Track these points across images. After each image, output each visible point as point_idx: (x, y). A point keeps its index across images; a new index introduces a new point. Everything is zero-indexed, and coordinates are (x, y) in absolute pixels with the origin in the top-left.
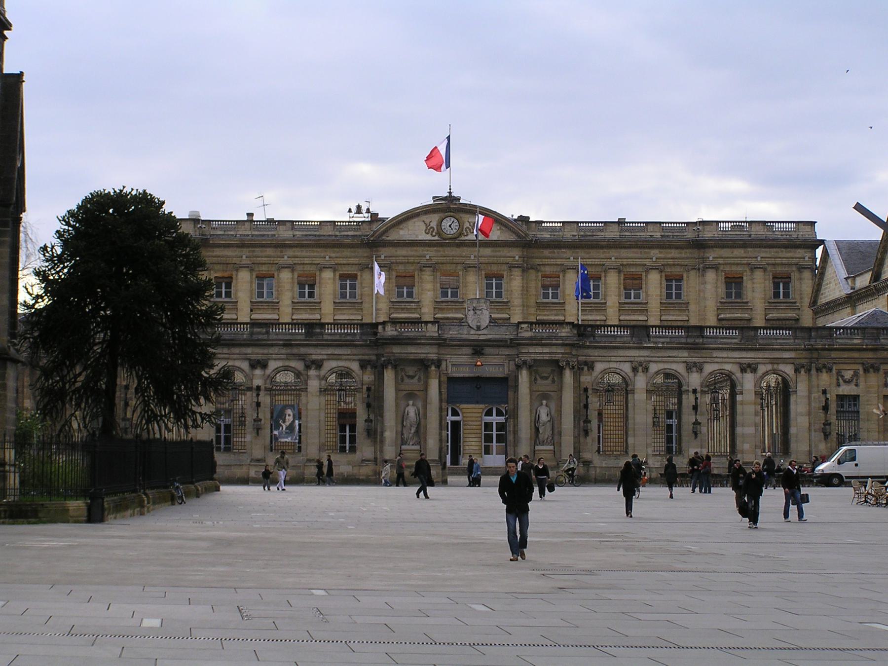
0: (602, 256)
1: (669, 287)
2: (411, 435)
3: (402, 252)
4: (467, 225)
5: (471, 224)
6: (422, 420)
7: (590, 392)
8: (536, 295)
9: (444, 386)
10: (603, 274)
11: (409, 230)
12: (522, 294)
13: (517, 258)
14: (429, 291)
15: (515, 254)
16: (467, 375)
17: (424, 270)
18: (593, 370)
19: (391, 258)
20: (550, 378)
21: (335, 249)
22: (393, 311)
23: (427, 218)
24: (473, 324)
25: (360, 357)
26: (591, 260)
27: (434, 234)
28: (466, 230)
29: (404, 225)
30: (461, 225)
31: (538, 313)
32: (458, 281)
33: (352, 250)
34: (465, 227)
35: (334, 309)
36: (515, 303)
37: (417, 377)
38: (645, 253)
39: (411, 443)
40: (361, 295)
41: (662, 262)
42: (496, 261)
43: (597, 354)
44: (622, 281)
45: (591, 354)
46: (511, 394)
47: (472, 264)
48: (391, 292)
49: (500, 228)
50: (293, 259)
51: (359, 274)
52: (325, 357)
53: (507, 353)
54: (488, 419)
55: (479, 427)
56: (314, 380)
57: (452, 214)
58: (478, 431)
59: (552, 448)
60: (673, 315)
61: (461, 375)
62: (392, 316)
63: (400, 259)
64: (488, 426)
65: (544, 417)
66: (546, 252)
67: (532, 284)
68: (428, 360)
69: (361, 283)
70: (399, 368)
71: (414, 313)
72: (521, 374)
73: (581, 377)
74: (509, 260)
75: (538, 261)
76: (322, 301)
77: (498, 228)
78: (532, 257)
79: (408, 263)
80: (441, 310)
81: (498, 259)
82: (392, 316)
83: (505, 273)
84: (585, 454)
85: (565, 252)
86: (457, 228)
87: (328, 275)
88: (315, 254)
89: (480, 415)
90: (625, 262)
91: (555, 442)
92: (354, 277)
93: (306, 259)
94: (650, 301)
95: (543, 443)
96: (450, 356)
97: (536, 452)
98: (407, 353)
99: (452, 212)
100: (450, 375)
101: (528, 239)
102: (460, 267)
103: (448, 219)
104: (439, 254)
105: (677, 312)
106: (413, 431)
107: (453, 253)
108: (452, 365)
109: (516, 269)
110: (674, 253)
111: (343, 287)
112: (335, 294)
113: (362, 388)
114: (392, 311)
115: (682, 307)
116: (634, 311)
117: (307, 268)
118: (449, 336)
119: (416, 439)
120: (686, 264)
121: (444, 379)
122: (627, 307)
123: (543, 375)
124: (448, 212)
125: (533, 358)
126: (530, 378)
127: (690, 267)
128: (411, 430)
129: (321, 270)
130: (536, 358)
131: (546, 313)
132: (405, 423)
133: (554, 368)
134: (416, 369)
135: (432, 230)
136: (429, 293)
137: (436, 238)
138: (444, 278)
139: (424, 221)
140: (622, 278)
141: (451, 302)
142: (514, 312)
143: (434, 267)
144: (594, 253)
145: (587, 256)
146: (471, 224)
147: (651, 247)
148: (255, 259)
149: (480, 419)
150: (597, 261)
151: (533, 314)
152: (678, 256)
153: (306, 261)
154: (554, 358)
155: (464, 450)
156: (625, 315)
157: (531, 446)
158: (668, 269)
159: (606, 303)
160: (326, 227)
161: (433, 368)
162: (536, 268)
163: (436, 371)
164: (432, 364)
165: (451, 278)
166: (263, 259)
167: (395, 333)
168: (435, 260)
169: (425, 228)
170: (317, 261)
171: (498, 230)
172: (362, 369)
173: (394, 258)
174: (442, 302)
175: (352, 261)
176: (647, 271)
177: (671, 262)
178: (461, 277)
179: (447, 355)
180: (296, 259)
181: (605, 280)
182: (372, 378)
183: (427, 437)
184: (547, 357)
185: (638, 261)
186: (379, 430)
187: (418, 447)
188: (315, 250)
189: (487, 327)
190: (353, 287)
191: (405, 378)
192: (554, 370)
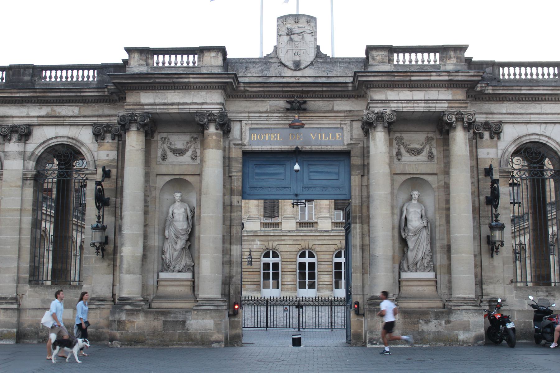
2: (176, 254)
6: (197, 228)
7: (496, 176)
9: (237, 166)
16: (276, 147)
18: (499, 138)
20: (425, 153)
24: (287, 59)
25: (95, 120)
37: (189, 153)
39: (177, 268)
43: (504, 111)
45: (495, 112)
46: (355, 179)
52: (35, 121)
53: (348, 108)
55: (330, 266)
56: (14, 159)
58: (330, 270)
59: (431, 275)
61: (267, 147)
65: (415, 222)
68: (201, 114)
70: (158, 137)
72: (374, 140)
73: (479, 150)
84: (491, 286)
89: (331, 256)
91: (438, 264)
95: (415, 267)
96: (247, 115)
97: (403, 283)
98: (165, 104)
100: (248, 148)
106: (179, 246)
108: (250, 129)
113: (96, 174)
118: (247, 80)
119: (185, 261)
121: (236, 153)
123: (412, 146)
125: (393, 109)
126: (390, 152)
128: (176, 243)
130: (401, 110)
132: (167, 233)
133: (429, 135)
134: (187, 138)
149: (330, 260)
154: (433, 110)
155: (318, 285)
157: (393, 272)
161: (212, 129)
163: (216, 134)
164: (210, 121)
167: (144, 69)
172: (97, 141)
179: (241, 112)
182: (113, 155)
183: (201, 255)
184: (420, 108)
186: (119, 244)
187: (188, 275)
189: (312, 64)
191: (169, 154)
192: (432, 138)
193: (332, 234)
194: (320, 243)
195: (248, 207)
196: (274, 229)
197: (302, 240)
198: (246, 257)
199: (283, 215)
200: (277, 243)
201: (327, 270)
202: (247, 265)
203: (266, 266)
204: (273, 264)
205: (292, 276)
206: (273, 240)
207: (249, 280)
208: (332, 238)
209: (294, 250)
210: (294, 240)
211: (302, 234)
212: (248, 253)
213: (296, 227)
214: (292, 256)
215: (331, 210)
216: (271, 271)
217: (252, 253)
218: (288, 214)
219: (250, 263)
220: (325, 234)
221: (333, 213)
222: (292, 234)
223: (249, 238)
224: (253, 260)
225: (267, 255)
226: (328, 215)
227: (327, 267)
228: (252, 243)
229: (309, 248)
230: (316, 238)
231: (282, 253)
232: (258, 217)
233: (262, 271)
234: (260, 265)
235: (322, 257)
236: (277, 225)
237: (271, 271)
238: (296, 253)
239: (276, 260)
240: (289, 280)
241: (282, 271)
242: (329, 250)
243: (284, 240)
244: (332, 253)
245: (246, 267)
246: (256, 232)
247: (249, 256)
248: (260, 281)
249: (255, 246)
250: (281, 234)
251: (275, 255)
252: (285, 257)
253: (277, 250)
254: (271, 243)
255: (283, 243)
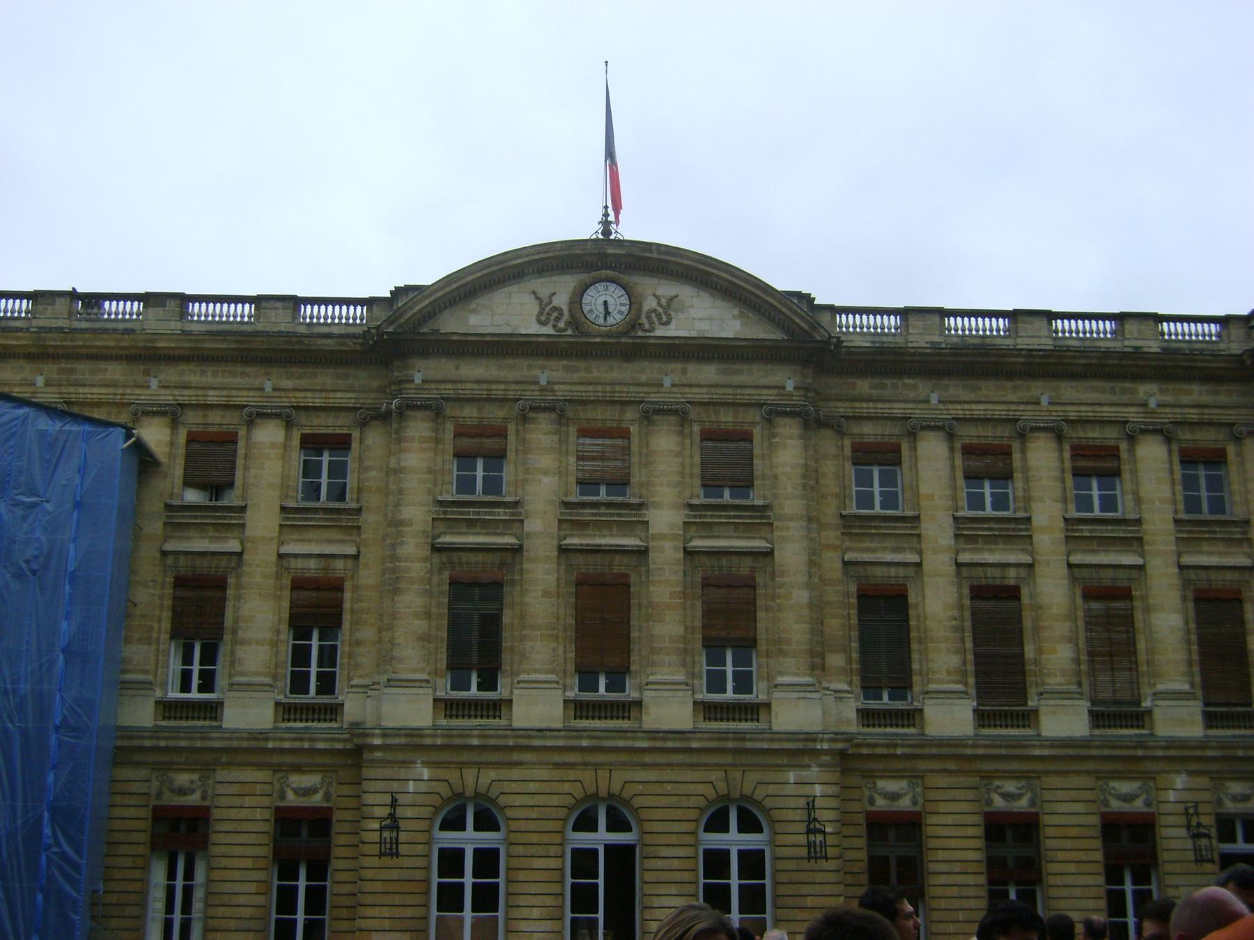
0: (1011, 397)
1: (1190, 483)
3: (473, 370)
4: (650, 304)
5: (663, 301)
8: (838, 496)
10: (1016, 445)
11: (493, 315)
12: (804, 486)
13: (790, 386)
14: (546, 473)
15: (787, 380)
17: (534, 418)
19: (442, 386)
21: (294, 370)
22: (441, 529)
23: (543, 286)
26: (981, 407)
27: (561, 325)
28: (648, 317)
29: (481, 301)
30: (634, 301)
31: (847, 544)
32: (626, 451)
33: (341, 371)
34: (646, 308)
35: (281, 525)
36: (788, 510)
38: (1123, 391)
40: (360, 490)
41: (1169, 414)
42: (730, 398)
44: (1068, 464)
47: (664, 403)
48: (440, 477)
49: (742, 312)
50: (176, 392)
51: (356, 434)
54: (715, 840)
57: (610, 273)
58: (687, 876)
60: (1211, 553)
62: (439, 540)
63: (469, 389)
64: (716, 862)
66: (863, 386)
67: (829, 468)
69: (360, 459)
71: (503, 534)
74: (768, 396)
75: (842, 408)
76: (249, 502)
77: (736, 312)
78: (827, 399)
79: (490, 400)
80: (581, 526)
81: (739, 391)
82: (439, 540)
83: (757, 432)
85: (914, 387)
86: (625, 309)
87: (269, 435)
88: (238, 380)
90: (1073, 412)
92: (341, 443)
93: (211, 393)
94: (1146, 516)
99: (611, 268)
101: (819, 338)
102: (631, 414)
103: (600, 286)
104: (576, 377)
105: (1221, 547)
107: (615, 375)
109: (787, 420)
110: (1196, 393)
111: (310, 469)
112: (284, 486)
114: (441, 527)
115: (1231, 532)
116: (1107, 543)
117: (215, 418)
120: (1232, 419)
122: (1086, 531)
124: (602, 268)
127: (1244, 429)
129: (251, 423)
131: (867, 545)
135: (555, 314)
136: (545, 480)
137: (569, 332)
138: (588, 441)
139: (534, 293)
140: (1067, 455)
141: (609, 505)
142: (783, 533)
143: (559, 410)
144: (989, 389)
145: (972, 397)
146: (663, 301)
147: (1141, 376)
148: (71, 390)
149: (689, 839)
150: (999, 411)
151: (835, 548)
152: (1207, 399)
153: (213, 397)
156: (1085, 551)
158: (1186, 435)
159: (1029, 519)
160: (273, 313)
162: (835, 426)
165: (608, 442)
166: (95, 390)
168: (562, 391)
169: (535, 309)
170: (243, 398)
171: (734, 317)
173: (450, 386)
174: (583, 505)
175: (340, 398)
176: (1132, 439)
177: (1193, 415)
178: (635, 438)
180: (187, 392)
181: (1024, 459)
185: (1107, 413)
188: (239, 369)
190: (338, 470)
193: (695, 745)
194: (651, 775)
195: (392, 642)
196: (484, 721)
197: (586, 764)
198: (376, 826)
199: (518, 674)
200: (492, 774)
201: (677, 876)
202: (381, 855)
203: (451, 861)
204: (477, 852)
205: (548, 901)
206: (479, 765)
207: (385, 912)
208: (695, 759)
209: (555, 800)
210: (557, 765)
211: (585, 743)
212: (384, 812)
213: (565, 718)
214: (551, 825)
215: (689, 659)
216: (468, 880)
217: (400, 812)
218: (536, 671)
219: (391, 850)
220: (670, 744)
221: (697, 670)
222: (549, 743)
223: (390, 756)
224: (403, 837)
225: (454, 823)
226: (680, 677)
227: (676, 864)
228: (403, 773)
229: (611, 796)
230: (636, 758)
231: (510, 813)
232: (424, 676)
233: (435, 880)
234: (428, 856)
235: (656, 827)
236: (496, 708)
237: (468, 880)
238: (562, 813)
239: (488, 839)
240: (536, 913)
241: (509, 881)
242: (684, 802)
243: (520, 764)
244: (694, 814)
245: (375, 862)
246: (415, 732)
247: (388, 822)
248: (426, 918)
249: (411, 786)
250: (511, 742)
251: (486, 821)
252: (522, 825)
253: (493, 801)
254: (470, 775)
255: (515, 773)
